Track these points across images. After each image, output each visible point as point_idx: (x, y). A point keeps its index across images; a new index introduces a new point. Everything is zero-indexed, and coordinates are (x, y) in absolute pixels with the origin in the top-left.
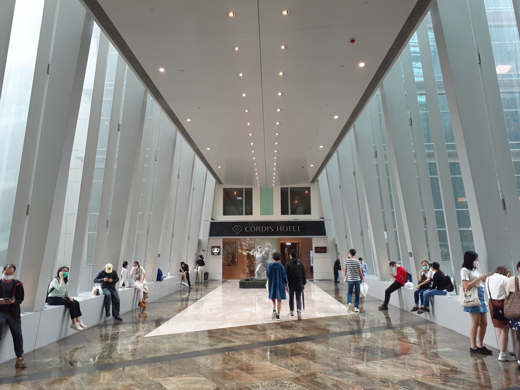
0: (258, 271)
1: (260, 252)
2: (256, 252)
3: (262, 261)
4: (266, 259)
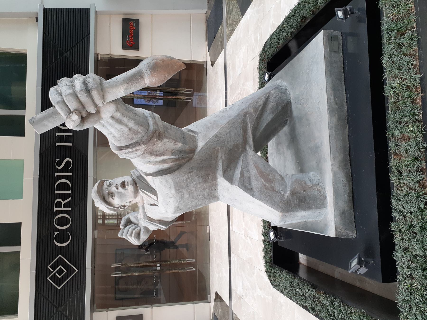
0: (274, 205)
1: (136, 192)
2: (140, 215)
3: (205, 179)
4: (193, 151)
